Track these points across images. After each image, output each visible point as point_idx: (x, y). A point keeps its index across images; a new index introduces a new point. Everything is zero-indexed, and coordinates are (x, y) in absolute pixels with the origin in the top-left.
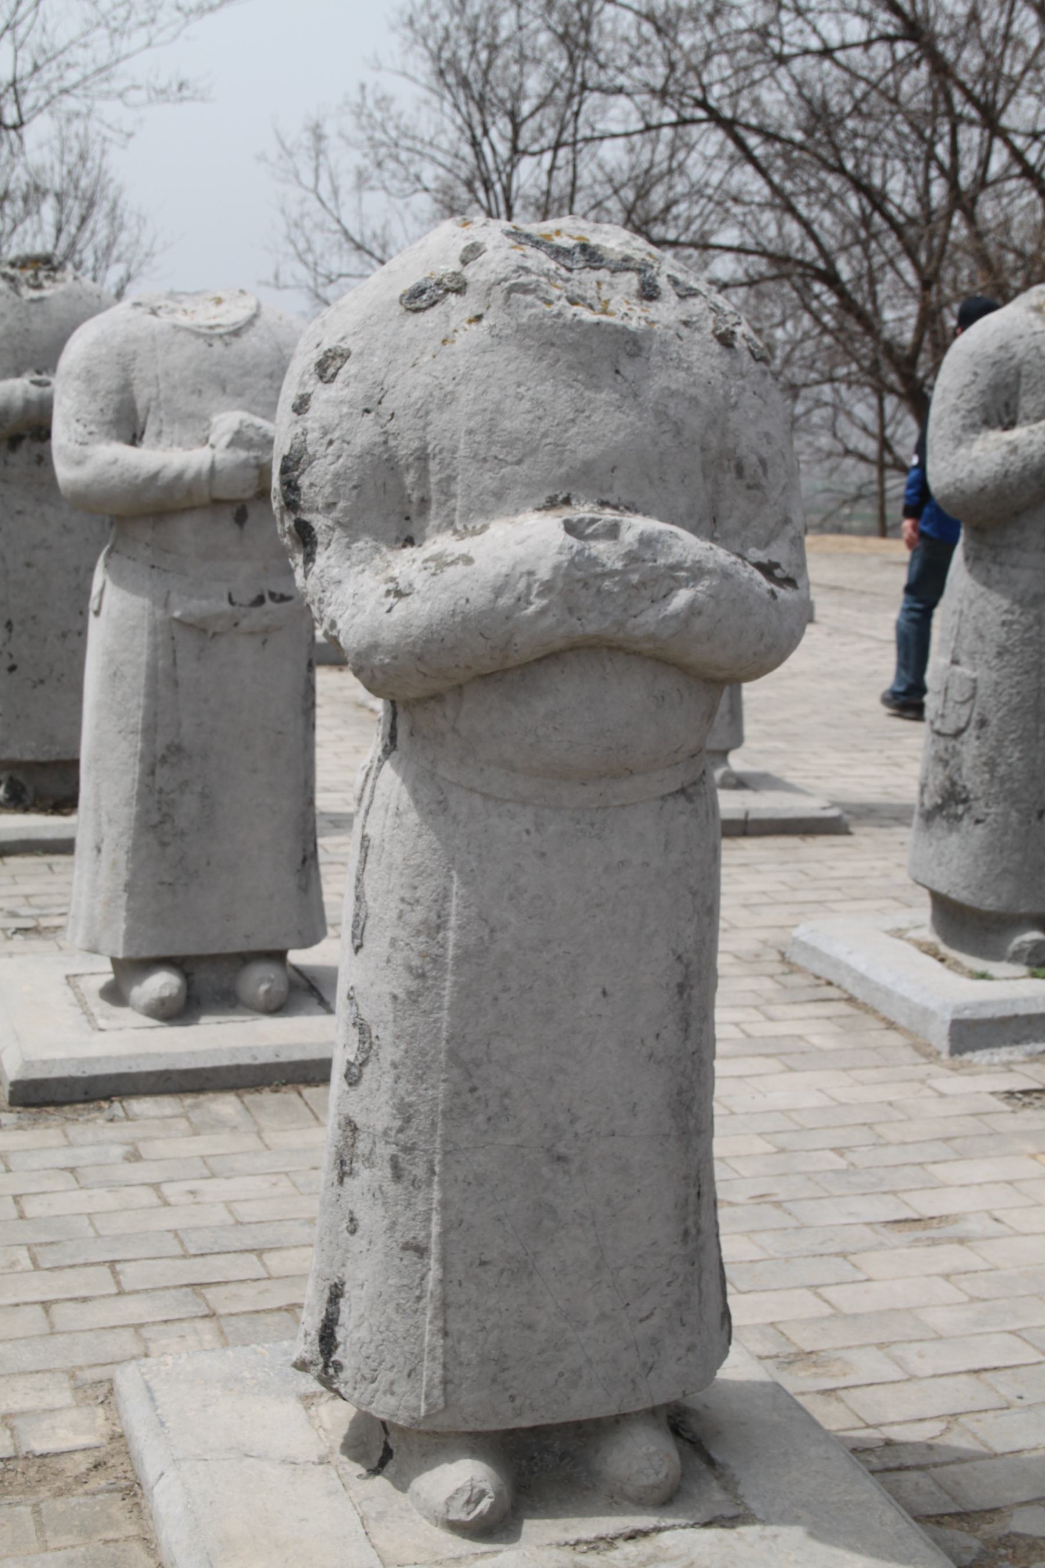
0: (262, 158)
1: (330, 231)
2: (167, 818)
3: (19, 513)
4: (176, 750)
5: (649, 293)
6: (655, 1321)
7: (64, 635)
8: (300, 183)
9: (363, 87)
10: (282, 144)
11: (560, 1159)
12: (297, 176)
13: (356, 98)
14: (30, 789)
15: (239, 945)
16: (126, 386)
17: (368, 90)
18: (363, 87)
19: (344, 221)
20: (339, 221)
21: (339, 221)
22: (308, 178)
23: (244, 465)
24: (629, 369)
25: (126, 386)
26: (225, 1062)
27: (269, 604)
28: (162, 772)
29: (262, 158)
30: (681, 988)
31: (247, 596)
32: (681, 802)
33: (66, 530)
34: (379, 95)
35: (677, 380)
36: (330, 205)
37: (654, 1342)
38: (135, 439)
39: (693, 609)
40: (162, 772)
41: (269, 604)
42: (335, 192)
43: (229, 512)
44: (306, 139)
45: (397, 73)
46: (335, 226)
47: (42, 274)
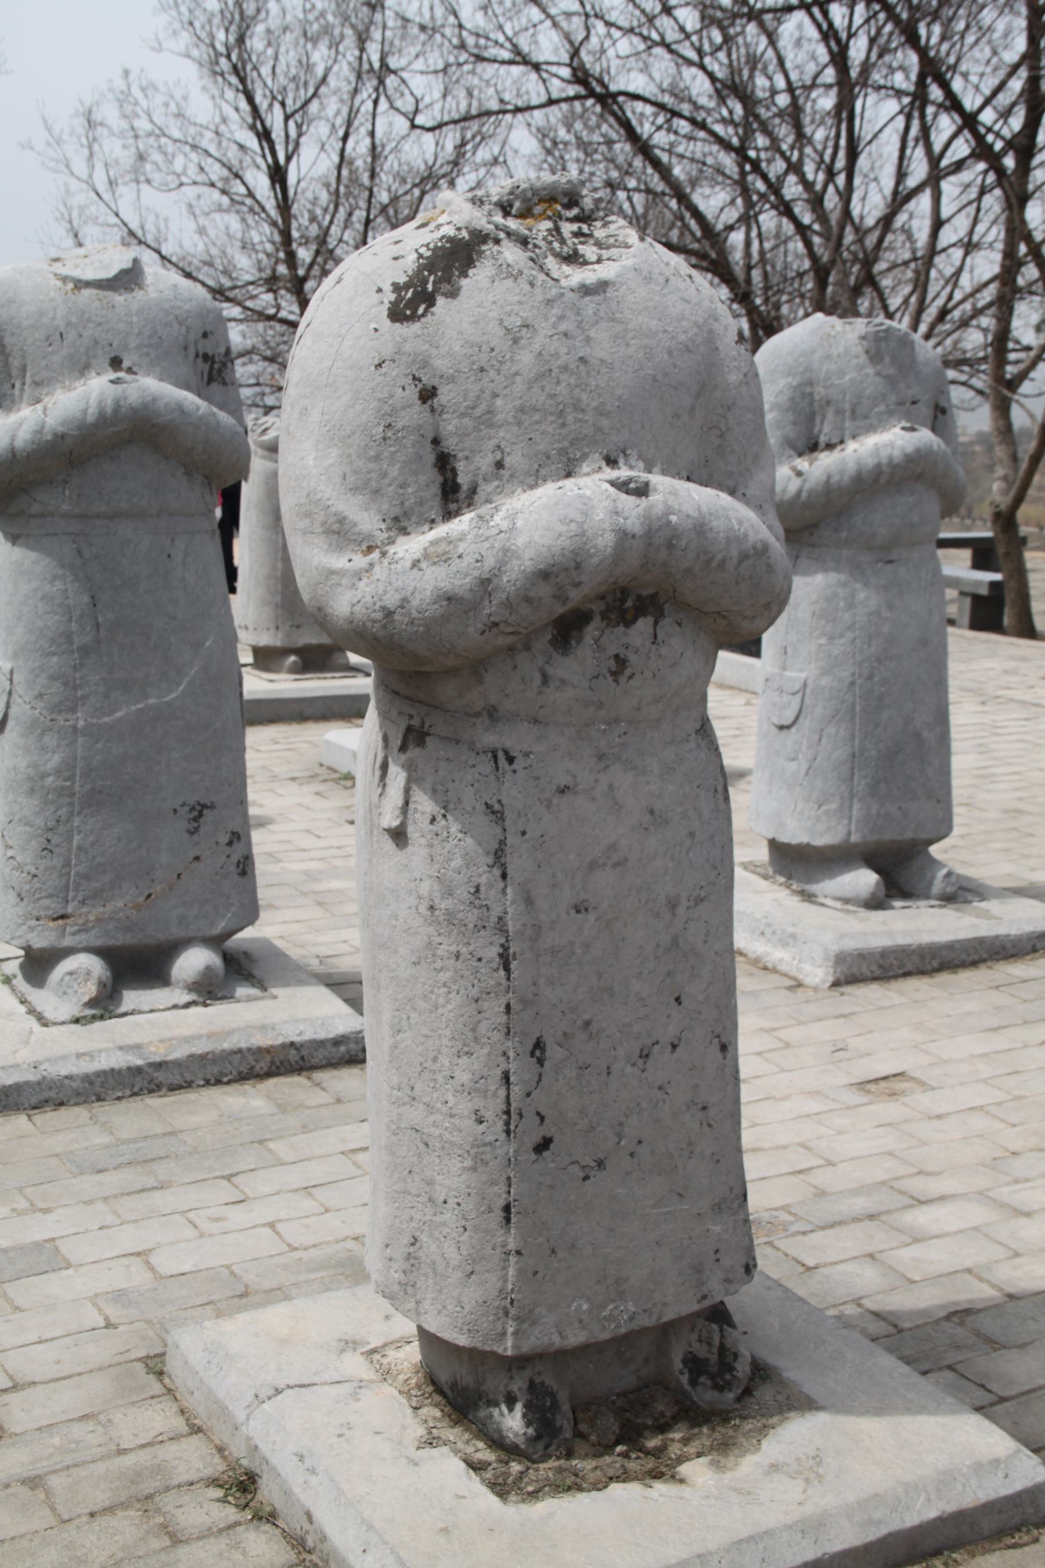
0: (27, 145)
1: (108, 225)
3: (563, 791)
8: (72, 174)
9: (126, 73)
10: (49, 129)
12: (68, 166)
13: (120, 84)
17: (132, 77)
18: (126, 73)
19: (121, 215)
20: (117, 215)
21: (117, 215)
22: (80, 167)
29: (27, 145)
33: (655, 817)
34: (144, 83)
36: (107, 196)
42: (112, 183)
44: (80, 125)
45: (180, 54)
46: (114, 220)
47: (567, 228)
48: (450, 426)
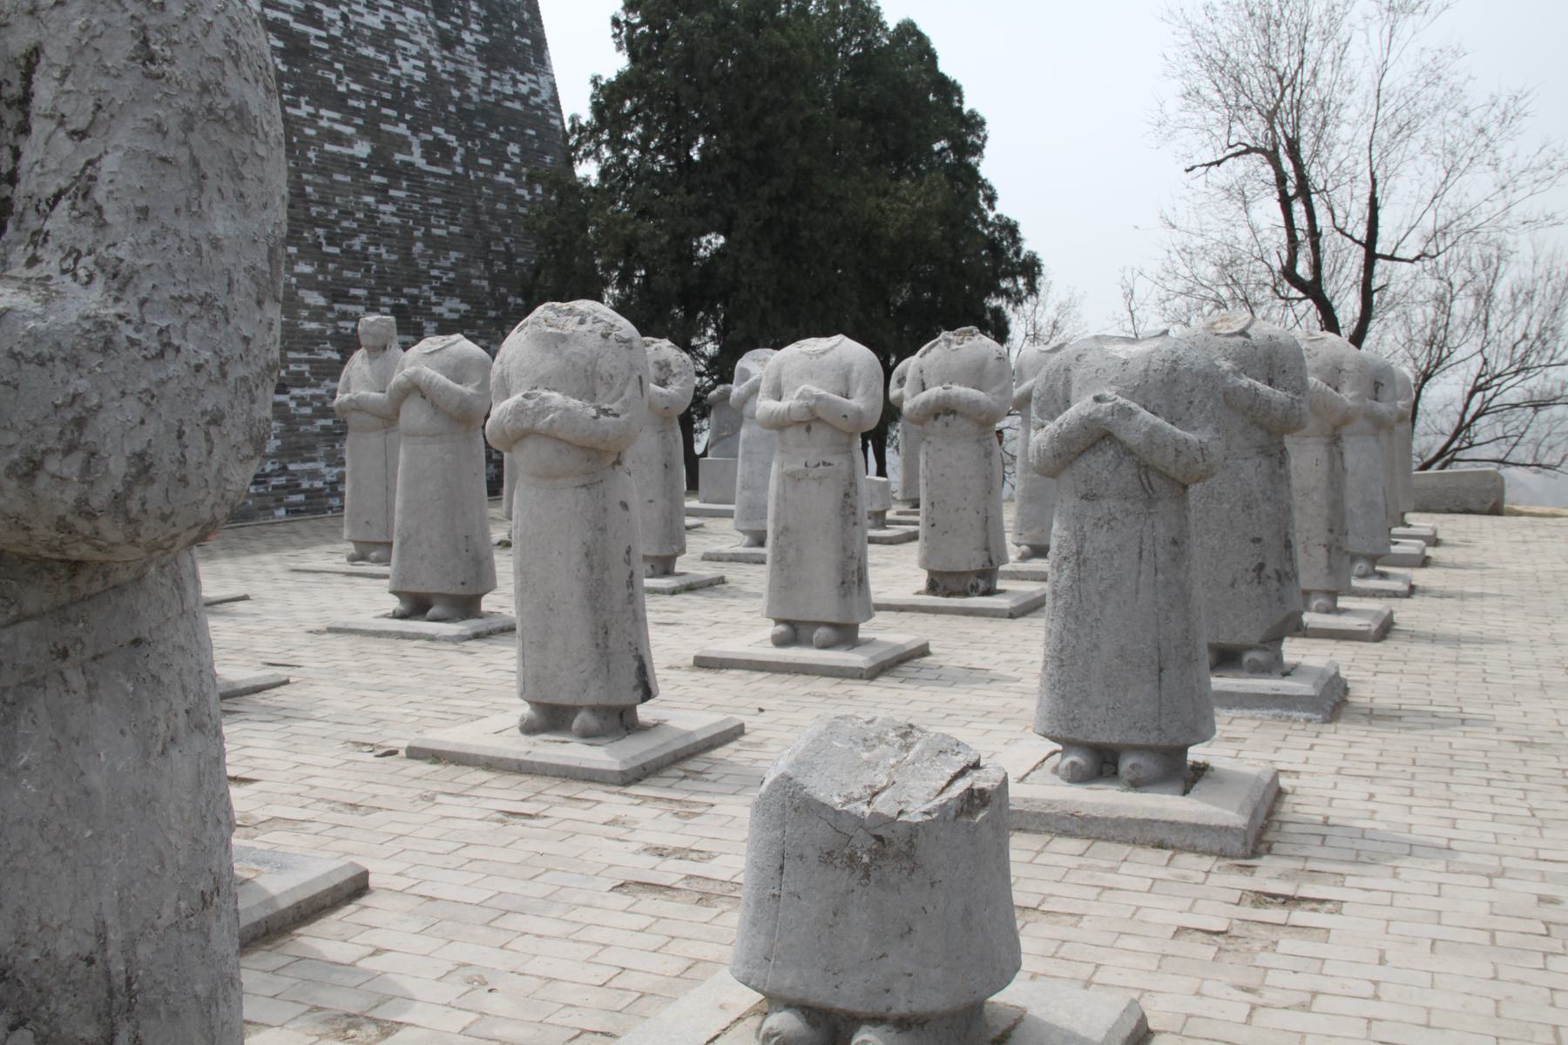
2: (783, 558)
4: (786, 529)
5: (582, 322)
6: (586, 674)
7: (957, 510)
11: (551, 609)
14: (941, 586)
15: (812, 618)
16: (778, 377)
23: (801, 406)
24: (561, 346)
25: (778, 377)
26: (773, 659)
27: (821, 467)
28: (781, 538)
30: (587, 555)
31: (812, 463)
32: (584, 490)
35: (578, 349)
37: (586, 682)
38: (780, 399)
39: (553, 421)
40: (781, 538)
41: (821, 467)
43: (803, 427)
48: (925, 378)
